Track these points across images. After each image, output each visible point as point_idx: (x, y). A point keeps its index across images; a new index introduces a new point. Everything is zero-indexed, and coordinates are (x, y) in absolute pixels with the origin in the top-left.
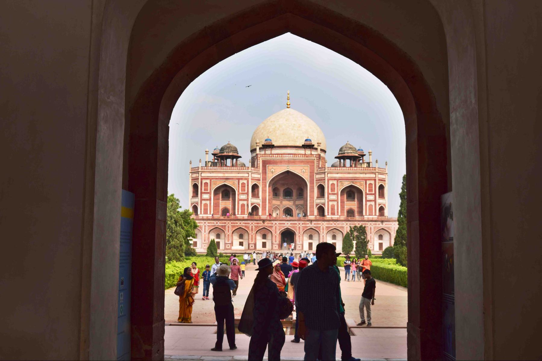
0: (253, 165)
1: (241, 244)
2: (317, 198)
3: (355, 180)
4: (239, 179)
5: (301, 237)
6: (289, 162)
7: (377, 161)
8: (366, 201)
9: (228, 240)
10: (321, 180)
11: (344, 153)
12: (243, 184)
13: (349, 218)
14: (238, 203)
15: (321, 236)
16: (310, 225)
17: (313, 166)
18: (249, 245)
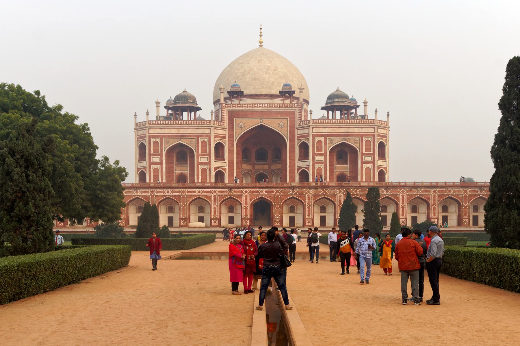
0: (217, 119)
1: (201, 219)
3: (348, 135)
4: (198, 137)
5: (280, 210)
7: (376, 111)
8: (363, 163)
9: (184, 216)
10: (305, 136)
11: (334, 102)
12: (204, 142)
13: (344, 184)
14: (198, 168)
16: (291, 193)
17: (294, 118)
18: (211, 220)
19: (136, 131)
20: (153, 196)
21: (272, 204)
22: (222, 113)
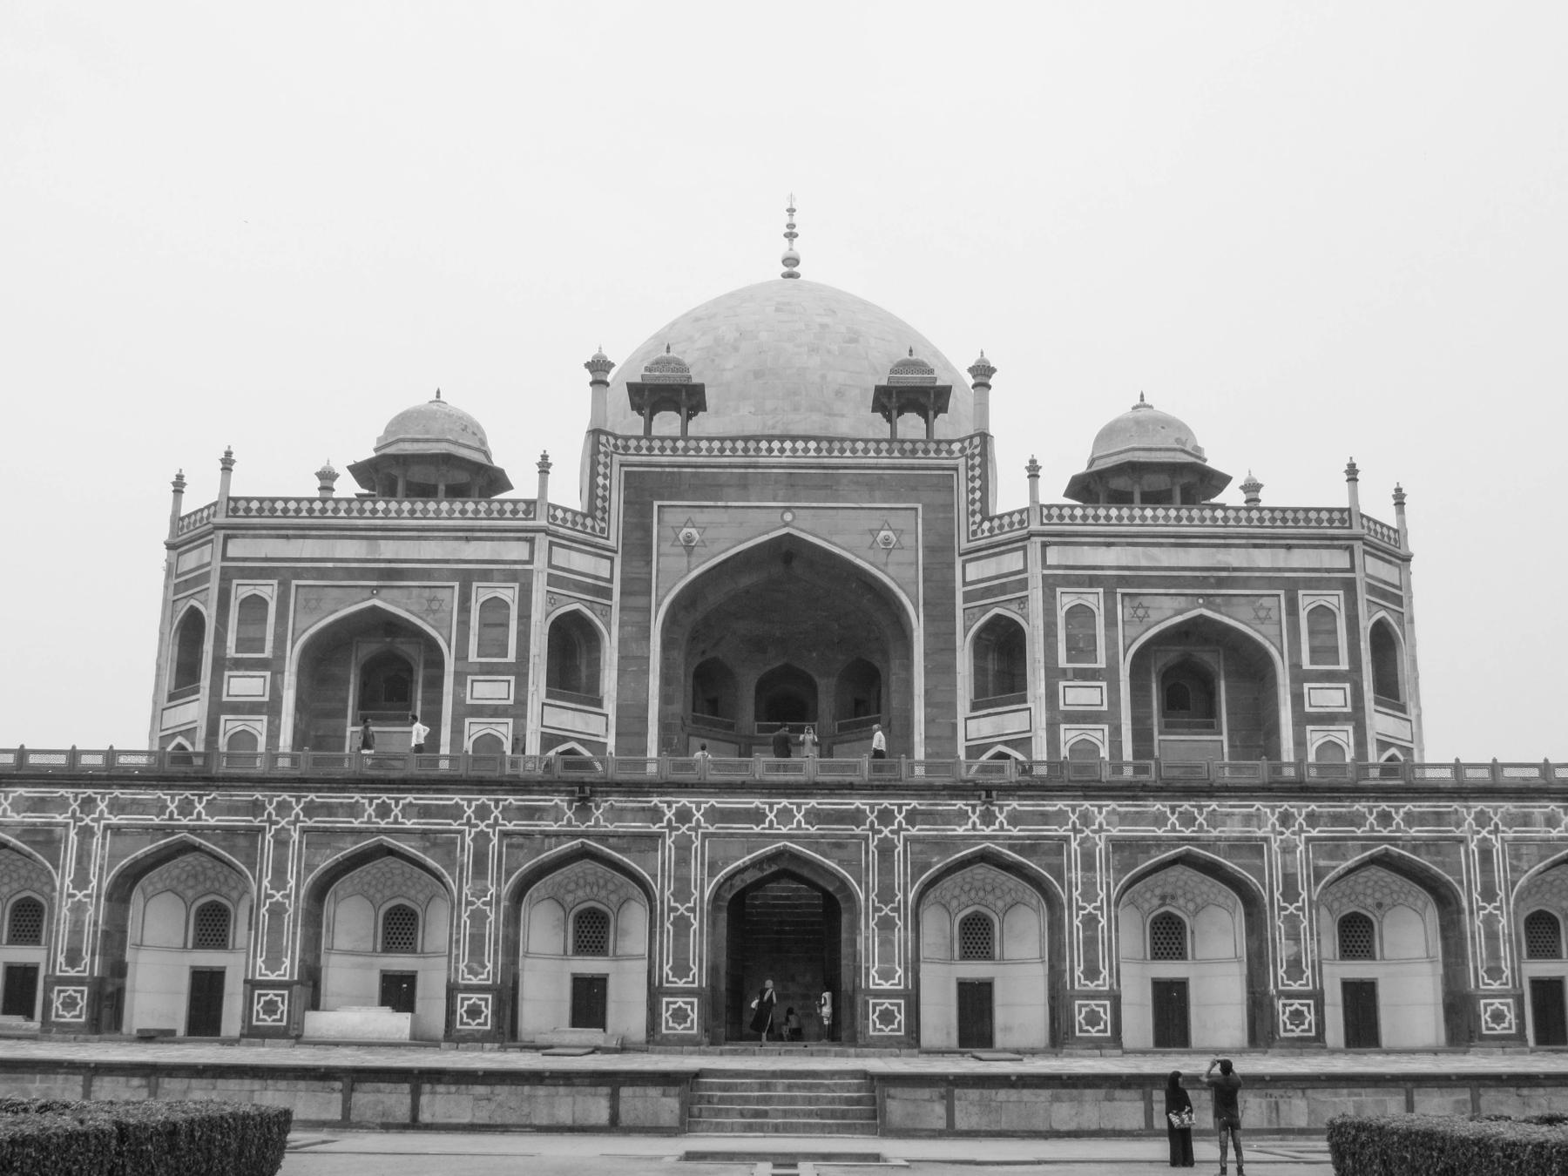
1: (398, 992)
2: (975, 707)
3: (1221, 583)
4: (467, 579)
5: (901, 934)
6: (795, 483)
7: (1352, 473)
8: (1303, 719)
9: (273, 962)
10: (1003, 589)
12: (495, 606)
14: (457, 731)
15: (1074, 923)
16: (972, 826)
17: (949, 507)
18: (452, 990)
19: (174, 553)
20: (86, 833)
21: (851, 897)
22: (594, 474)
